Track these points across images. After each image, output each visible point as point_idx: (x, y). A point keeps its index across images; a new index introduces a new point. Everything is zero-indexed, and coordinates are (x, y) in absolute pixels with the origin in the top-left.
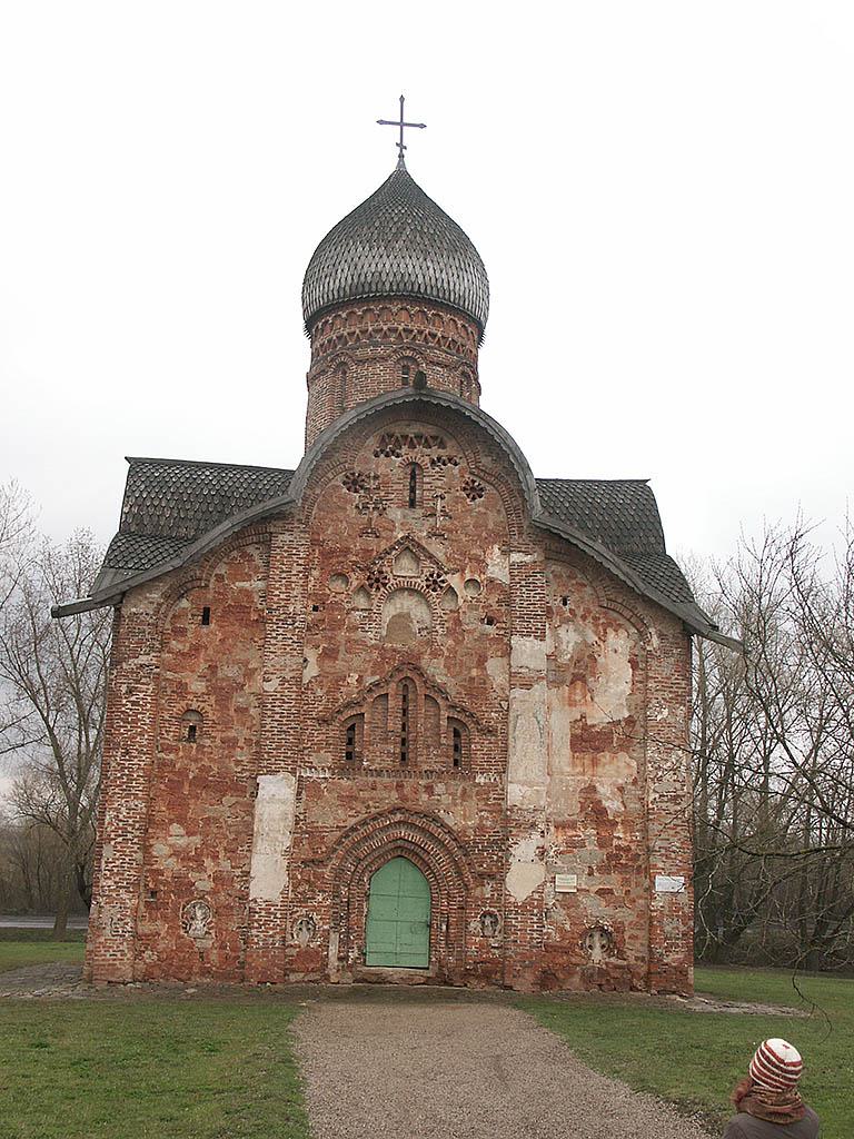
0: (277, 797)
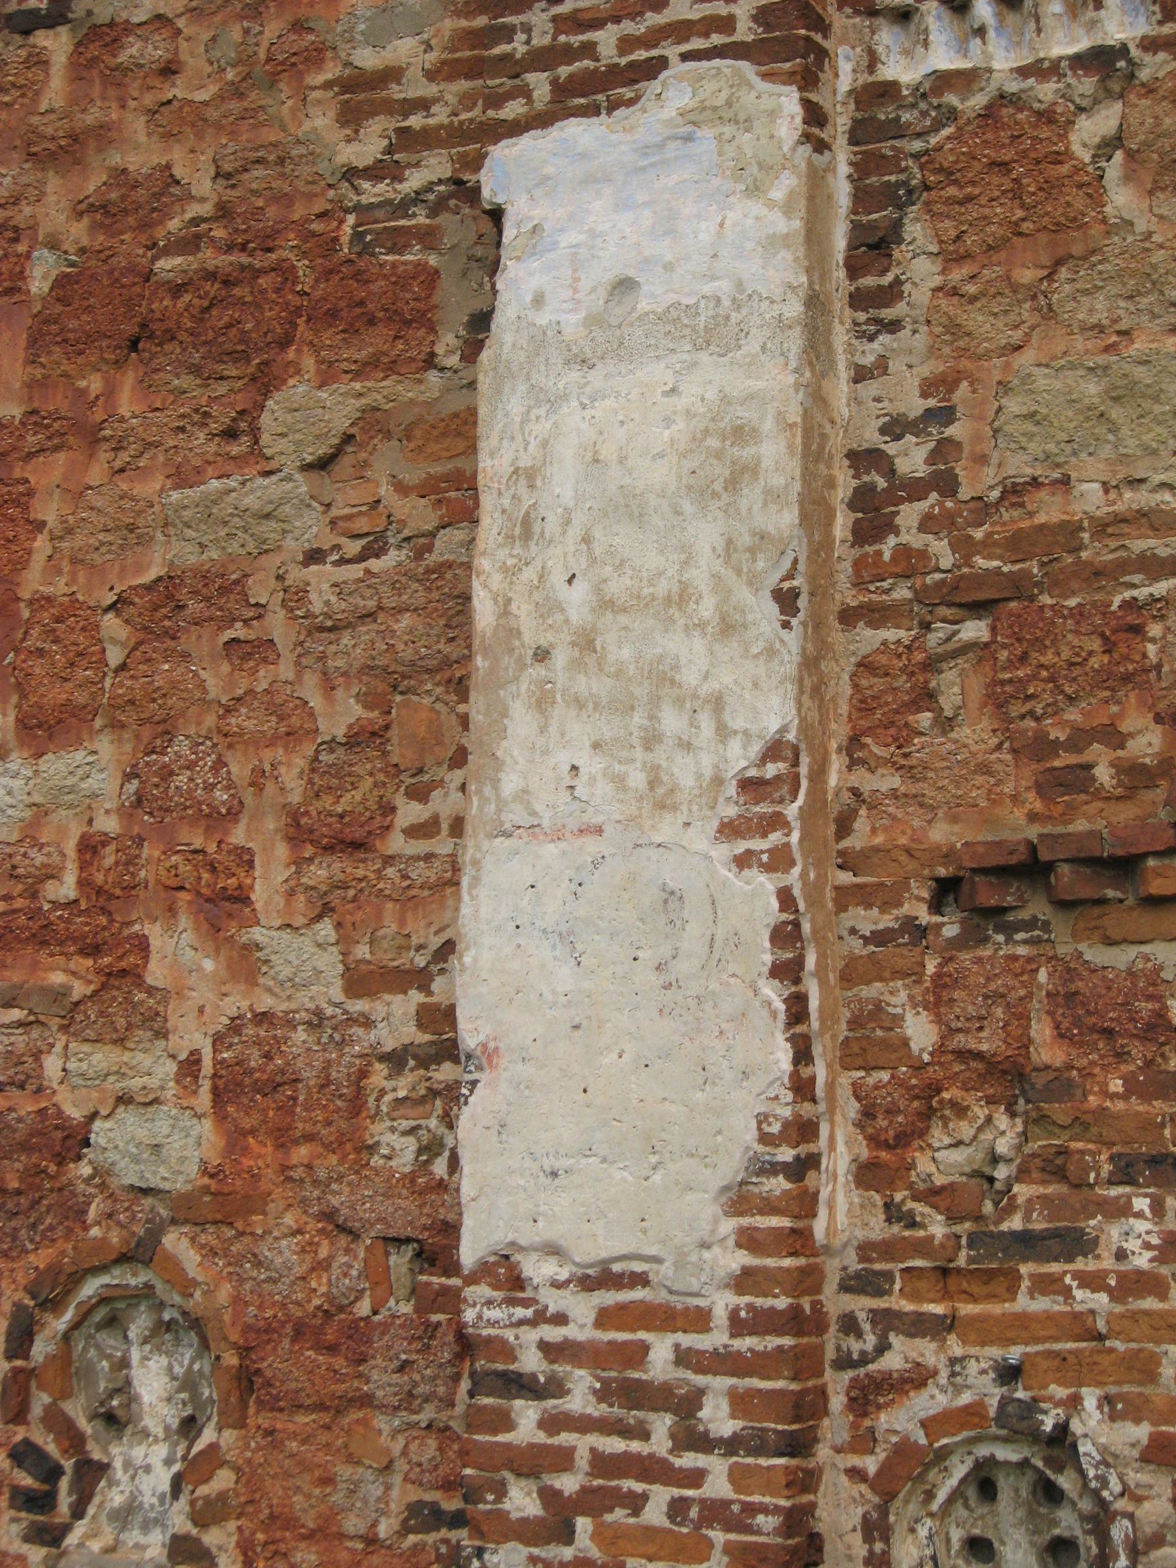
0: (653, 296)
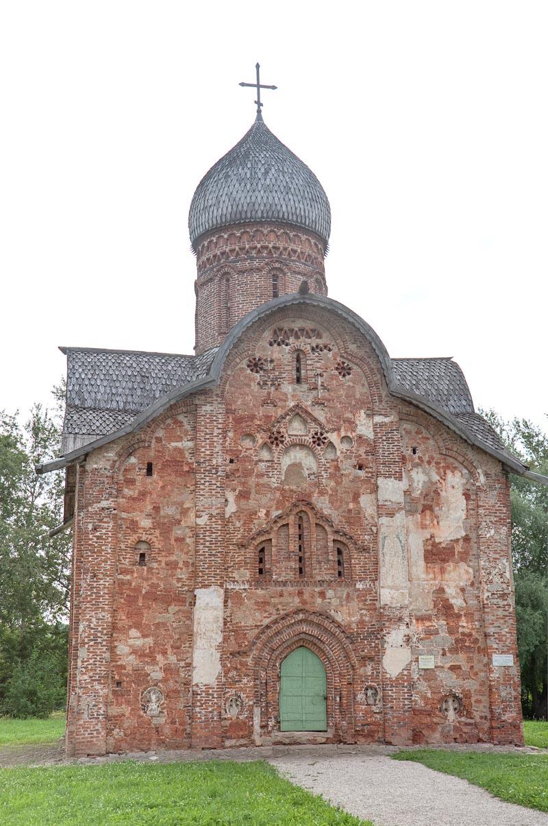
0: (210, 605)
